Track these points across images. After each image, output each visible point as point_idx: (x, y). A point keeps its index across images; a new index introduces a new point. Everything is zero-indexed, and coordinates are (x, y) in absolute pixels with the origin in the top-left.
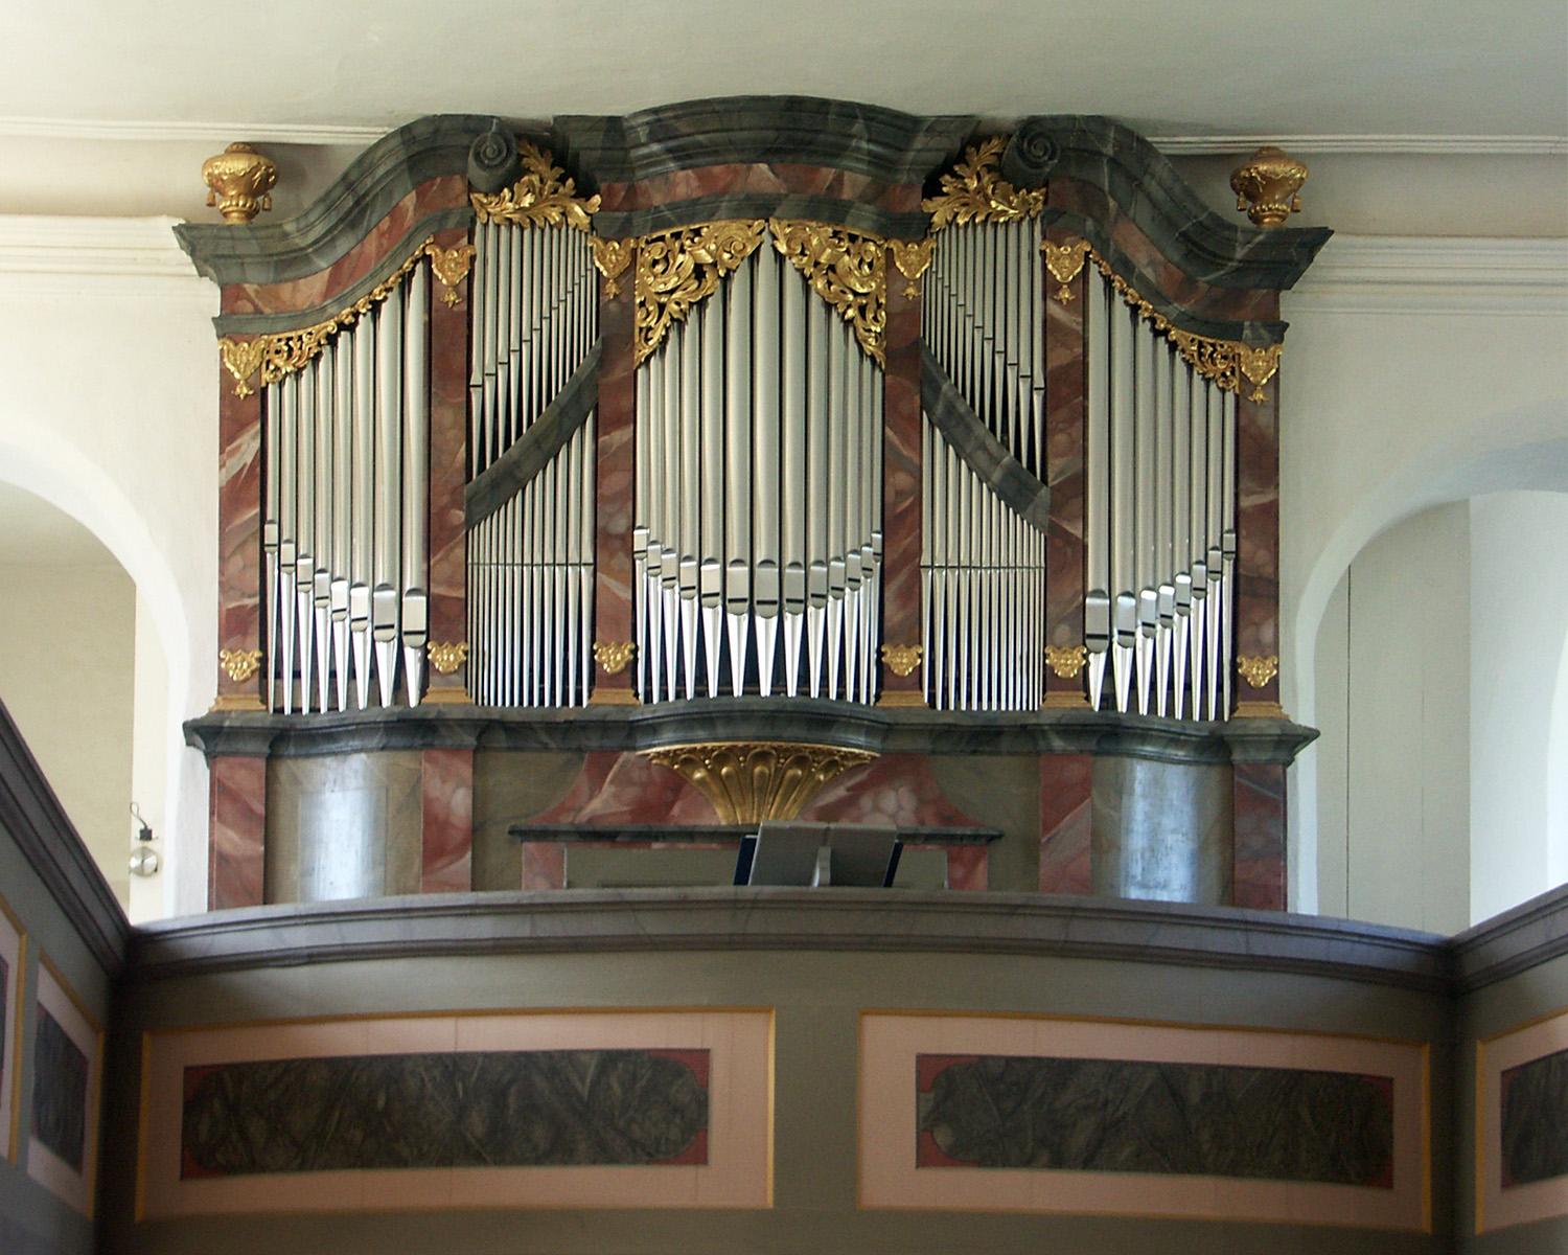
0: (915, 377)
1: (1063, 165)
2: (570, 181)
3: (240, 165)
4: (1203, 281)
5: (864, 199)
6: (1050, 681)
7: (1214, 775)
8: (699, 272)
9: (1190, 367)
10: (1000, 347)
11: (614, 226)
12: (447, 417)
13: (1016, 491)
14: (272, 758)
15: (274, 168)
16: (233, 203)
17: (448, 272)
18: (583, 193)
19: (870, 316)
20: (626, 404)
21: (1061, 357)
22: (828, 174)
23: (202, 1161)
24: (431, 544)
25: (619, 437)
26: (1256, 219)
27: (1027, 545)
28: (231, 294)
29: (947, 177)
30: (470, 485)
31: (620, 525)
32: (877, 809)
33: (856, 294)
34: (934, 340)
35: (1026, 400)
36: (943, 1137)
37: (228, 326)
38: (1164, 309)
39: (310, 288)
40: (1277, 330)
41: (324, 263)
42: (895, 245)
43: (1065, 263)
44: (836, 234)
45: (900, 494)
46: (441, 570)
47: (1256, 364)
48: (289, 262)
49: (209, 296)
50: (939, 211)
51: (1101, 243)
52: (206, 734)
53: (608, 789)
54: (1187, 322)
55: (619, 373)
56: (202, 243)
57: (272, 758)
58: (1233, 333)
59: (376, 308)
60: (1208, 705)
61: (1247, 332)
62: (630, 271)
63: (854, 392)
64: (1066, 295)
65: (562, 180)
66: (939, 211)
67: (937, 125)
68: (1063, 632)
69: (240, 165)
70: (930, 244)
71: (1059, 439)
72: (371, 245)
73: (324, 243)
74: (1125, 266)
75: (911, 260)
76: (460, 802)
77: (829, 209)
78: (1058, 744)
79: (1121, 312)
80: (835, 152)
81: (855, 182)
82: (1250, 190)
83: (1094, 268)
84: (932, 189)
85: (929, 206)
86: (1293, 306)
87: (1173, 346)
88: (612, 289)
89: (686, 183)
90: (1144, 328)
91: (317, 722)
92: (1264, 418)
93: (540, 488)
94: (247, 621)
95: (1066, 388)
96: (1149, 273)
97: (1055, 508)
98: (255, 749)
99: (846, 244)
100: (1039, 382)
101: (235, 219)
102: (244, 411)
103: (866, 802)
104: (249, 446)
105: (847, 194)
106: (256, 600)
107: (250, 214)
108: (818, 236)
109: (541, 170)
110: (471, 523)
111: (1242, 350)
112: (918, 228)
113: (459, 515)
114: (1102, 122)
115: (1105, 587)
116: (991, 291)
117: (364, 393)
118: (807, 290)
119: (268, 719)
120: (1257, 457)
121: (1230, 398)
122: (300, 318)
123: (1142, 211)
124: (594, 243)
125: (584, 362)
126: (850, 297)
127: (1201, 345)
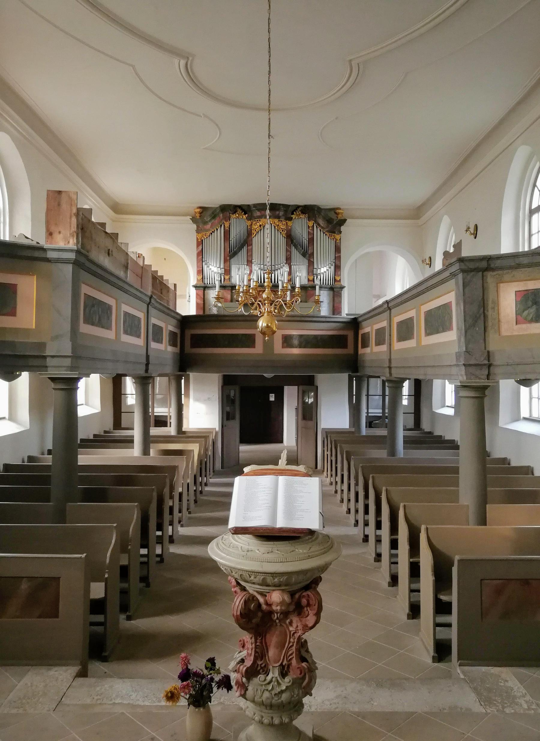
0: (291, 239)
1: (310, 211)
3: (199, 210)
5: (283, 215)
6: (309, 280)
8: (260, 226)
11: (249, 219)
12: (227, 245)
13: (304, 255)
14: (204, 290)
15: (203, 210)
16: (198, 215)
17: (227, 224)
18: (245, 214)
21: (310, 237)
22: (277, 212)
24: (225, 261)
25: (250, 248)
26: (337, 217)
27: (306, 261)
28: (198, 227)
30: (230, 254)
34: (293, 234)
35: (306, 242)
37: (198, 231)
39: (208, 226)
41: (210, 223)
43: (311, 224)
46: (226, 265)
47: (338, 237)
48: (205, 223)
49: (195, 226)
51: (316, 221)
52: (196, 287)
54: (328, 231)
55: (250, 239)
56: (194, 220)
57: (204, 290)
59: (217, 229)
63: (282, 241)
68: (310, 274)
69: (199, 210)
71: (310, 248)
72: (216, 221)
73: (211, 220)
74: (319, 224)
75: (290, 223)
76: (229, 297)
80: (279, 210)
81: (281, 213)
82: (336, 213)
84: (293, 214)
85: (292, 216)
86: (343, 228)
88: (249, 227)
89: (258, 214)
90: (322, 232)
91: (210, 286)
92: (339, 244)
93: (239, 254)
94: (201, 271)
95: (311, 241)
97: (310, 257)
101: (198, 217)
102: (200, 243)
104: (200, 247)
107: (200, 216)
109: (239, 211)
110: (230, 259)
112: (290, 219)
113: (228, 258)
116: (300, 226)
119: (203, 285)
122: (207, 230)
124: (246, 221)
125: (245, 237)
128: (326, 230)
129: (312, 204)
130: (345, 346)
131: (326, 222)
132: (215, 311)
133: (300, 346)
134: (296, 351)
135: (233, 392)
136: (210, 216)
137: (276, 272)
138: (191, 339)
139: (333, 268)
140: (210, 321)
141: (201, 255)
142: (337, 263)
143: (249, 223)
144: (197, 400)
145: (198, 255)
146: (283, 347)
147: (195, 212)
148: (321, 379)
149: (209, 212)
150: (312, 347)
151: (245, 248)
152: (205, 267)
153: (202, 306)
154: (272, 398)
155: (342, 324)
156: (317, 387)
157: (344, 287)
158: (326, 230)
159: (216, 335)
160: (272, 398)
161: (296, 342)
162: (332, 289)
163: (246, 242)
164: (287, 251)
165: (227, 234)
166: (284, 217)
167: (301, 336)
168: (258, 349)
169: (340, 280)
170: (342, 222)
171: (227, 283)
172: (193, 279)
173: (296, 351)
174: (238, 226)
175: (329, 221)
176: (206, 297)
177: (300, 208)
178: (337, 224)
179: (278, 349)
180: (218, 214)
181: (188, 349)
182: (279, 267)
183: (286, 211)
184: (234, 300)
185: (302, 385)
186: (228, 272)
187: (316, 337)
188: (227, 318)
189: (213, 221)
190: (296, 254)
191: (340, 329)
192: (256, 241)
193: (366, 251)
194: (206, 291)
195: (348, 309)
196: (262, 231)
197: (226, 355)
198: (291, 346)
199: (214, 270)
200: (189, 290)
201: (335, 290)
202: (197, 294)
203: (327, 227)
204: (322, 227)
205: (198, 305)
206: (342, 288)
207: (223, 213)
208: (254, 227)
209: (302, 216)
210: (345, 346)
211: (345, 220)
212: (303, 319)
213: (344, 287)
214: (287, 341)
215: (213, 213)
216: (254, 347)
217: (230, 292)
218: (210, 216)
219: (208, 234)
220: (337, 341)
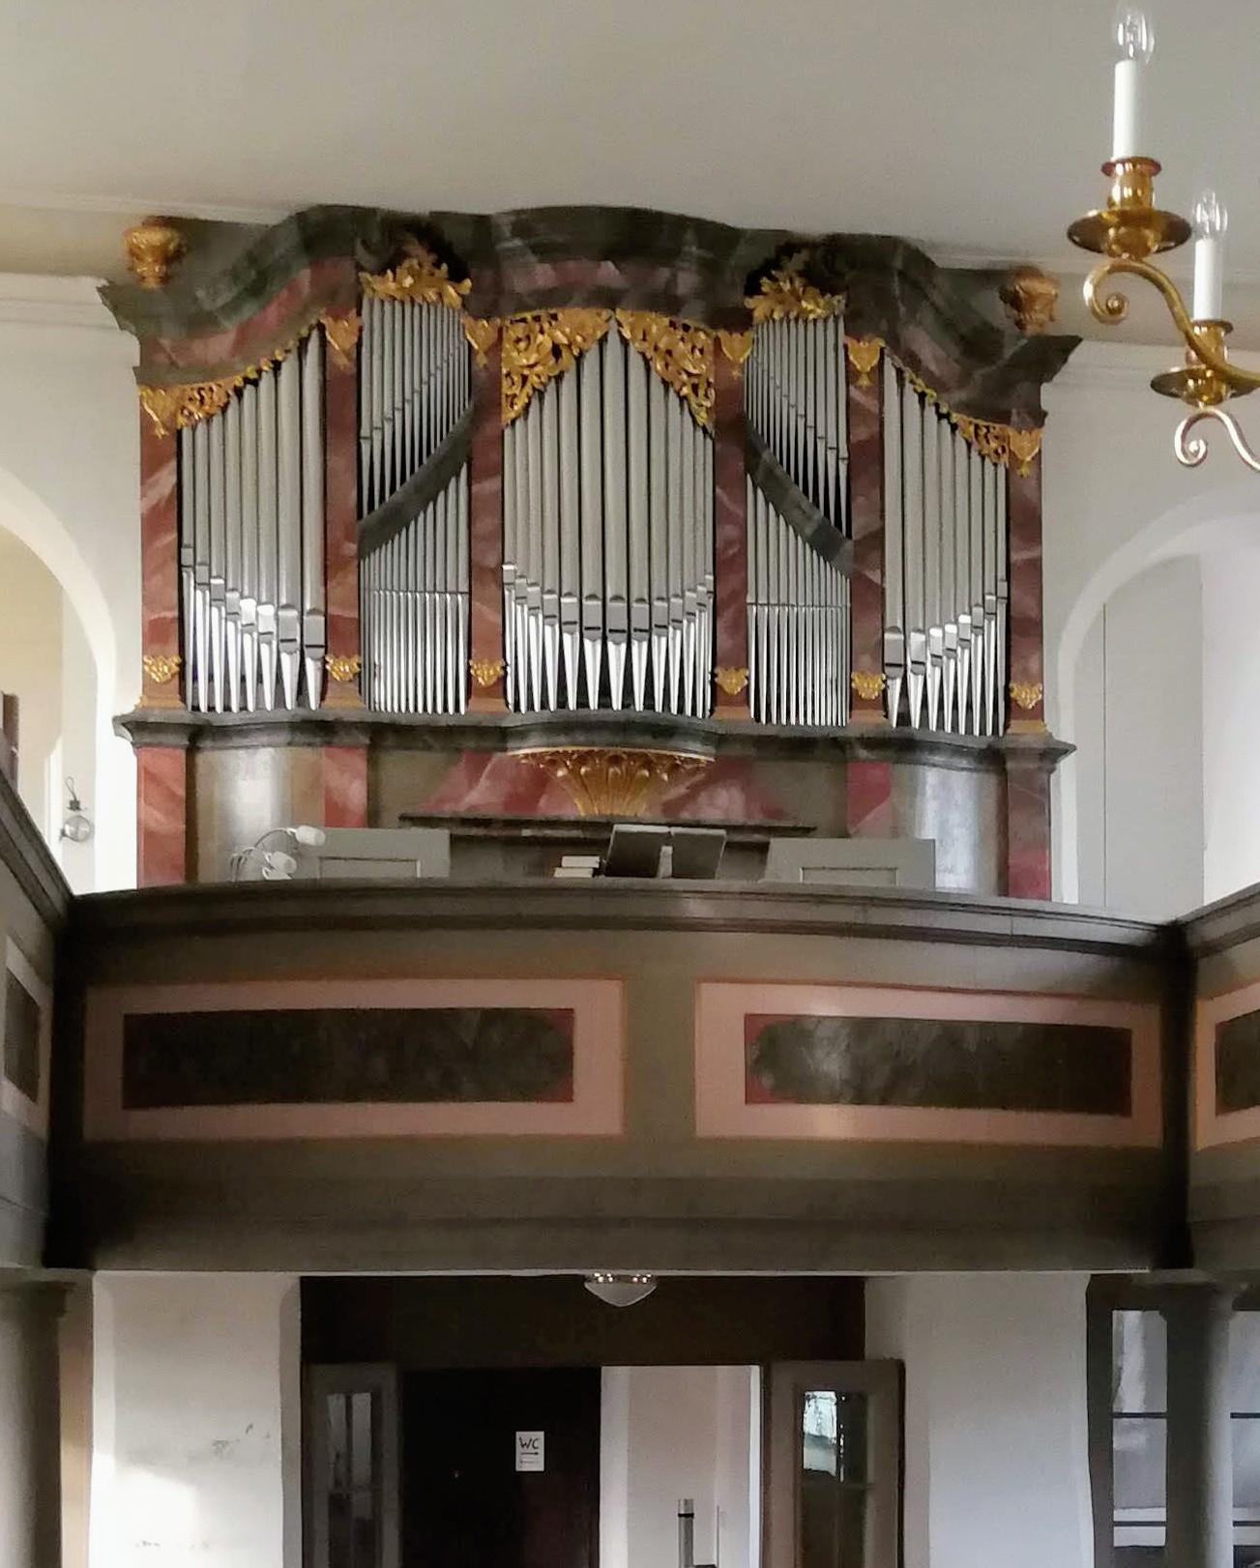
0: (740, 441)
1: (862, 275)
2: (444, 267)
3: (156, 237)
4: (978, 374)
5: (699, 295)
6: (854, 700)
7: (991, 781)
8: (556, 351)
9: (969, 445)
10: (810, 422)
11: (486, 305)
12: (341, 463)
13: (825, 544)
14: (192, 751)
15: (188, 239)
16: (150, 270)
17: (340, 339)
18: (456, 277)
19: (701, 392)
20: (494, 456)
21: (862, 433)
22: (664, 273)
23: (140, 1093)
24: (328, 570)
25: (487, 486)
26: (1020, 324)
27: (835, 586)
28: (149, 348)
29: (764, 280)
30: (364, 522)
31: (491, 561)
32: (711, 804)
33: (689, 374)
34: (756, 415)
35: (832, 465)
36: (767, 1081)
37: (148, 375)
38: (945, 396)
39: (218, 346)
40: (1038, 417)
41: (230, 328)
42: (722, 334)
43: (865, 354)
44: (672, 324)
45: (729, 544)
46: (336, 592)
47: (1022, 443)
48: (200, 323)
49: (128, 347)
50: (759, 306)
51: (894, 341)
52: (136, 727)
53: (484, 782)
54: (966, 408)
55: (489, 430)
56: (124, 301)
57: (192, 751)
58: (1004, 418)
59: (277, 366)
60: (980, 730)
61: (1014, 418)
62: (496, 347)
63: (688, 456)
64: (864, 382)
65: (437, 265)
66: (759, 306)
67: (759, 236)
68: (865, 660)
69: (156, 237)
70: (750, 334)
71: (859, 501)
72: (272, 312)
73: (233, 307)
74: (913, 361)
75: (736, 346)
76: (356, 793)
77: (667, 303)
78: (863, 753)
79: (912, 401)
80: (670, 256)
81: (687, 281)
82: (1014, 301)
83: (887, 360)
84: (753, 289)
85: (750, 303)
86: (1049, 395)
87: (954, 427)
88: (481, 360)
89: (543, 275)
90: (930, 411)
91: (229, 720)
92: (1029, 492)
93: (423, 522)
94: (168, 632)
95: (866, 457)
96: (933, 367)
97: (859, 557)
98: (182, 738)
99: (680, 333)
100: (844, 453)
101: (152, 284)
102: (162, 450)
103: (703, 797)
104: (166, 479)
106: (176, 613)
107: (165, 279)
108: (657, 324)
109: (418, 255)
110: (362, 555)
111: (1011, 432)
112: (742, 321)
113: (352, 548)
115: (900, 625)
117: (267, 440)
118: (648, 370)
119: (187, 717)
120: (1023, 521)
121: (1002, 471)
122: (211, 372)
123: (927, 316)
124: (466, 320)
125: (459, 421)
126: (684, 377)
127: (977, 427)
128: (960, 395)
129: (875, 230)
130: (1112, 1097)
131: (956, 352)
132: (277, 867)
133: (859, 1094)
134: (831, 1122)
135: (358, 1413)
136: (235, 275)
137: (659, 645)
138: (131, 1050)
139: (995, 630)
140: (268, 925)
141: (167, 525)
142: (1023, 602)
143: (481, 333)
144: (139, 1454)
145: (152, 524)
146: (753, 1095)
147: (134, 253)
148: (929, 1312)
149: (225, 257)
150: (925, 1100)
151: (457, 493)
152: (197, 601)
153: (179, 848)
154: (531, 1454)
155: (1079, 960)
156: (900, 1368)
157: (1066, 750)
158: (960, 395)
159: (305, 1021)
160: (531, 1454)
161: (831, 1064)
162: (993, 758)
163: (466, 447)
164: (719, 515)
165: (341, 403)
166: (698, 306)
167: (863, 1028)
168: (594, 1107)
169: (1040, 704)
170: (1051, 354)
171: (344, 706)
172: (114, 674)
173: (831, 1122)
174: (410, 352)
175: (976, 345)
176: (201, 791)
177: (799, 260)
178: (1017, 362)
179: (723, 1105)
180: (286, 269)
181: (106, 1115)
182: (676, 614)
183: (710, 269)
184: (385, 817)
185: (796, 1355)
186: (345, 634)
187: (951, 1032)
188: (386, 907)
189: (249, 310)
190: (776, 547)
191: (1094, 992)
192: (528, 452)
193: (1157, 555)
194: (201, 759)
195: (1103, 875)
196: (568, 386)
197: (377, 1146)
198: (799, 1089)
199: (250, 635)
200: (85, 762)
201: (1014, 769)
202: (147, 778)
203: (963, 381)
204: (934, 382)
205: (148, 838)
206: (1053, 753)
207: (315, 264)
208: (518, 358)
209: (813, 306)
210: (1112, 1097)
211: (1067, 345)
212: (879, 917)
213: (1066, 750)
214: (777, 1056)
215: (252, 259)
216: (567, 1096)
217: (359, 763)
218: (235, 275)
219: (218, 397)
220: (1064, 1065)
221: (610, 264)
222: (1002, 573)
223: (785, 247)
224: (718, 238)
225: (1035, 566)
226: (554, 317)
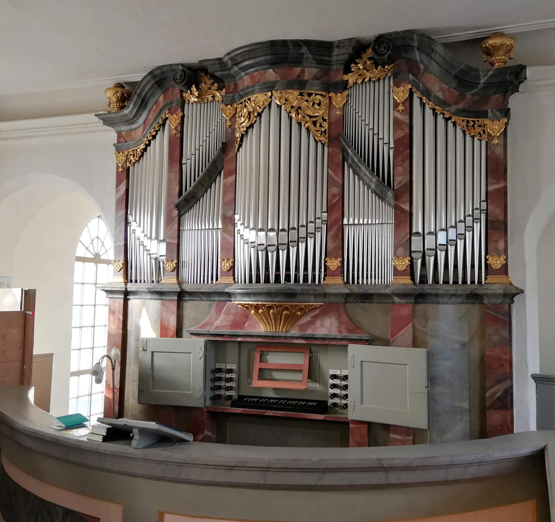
0: (340, 146)
4: (469, 95)
10: (376, 132)
11: (229, 101)
19: (318, 125)
20: (233, 166)
21: (401, 134)
27: (388, 214)
29: (353, 65)
31: (230, 213)
32: (322, 326)
33: (311, 117)
35: (387, 152)
38: (447, 109)
40: (506, 113)
42: (332, 94)
43: (401, 94)
44: (301, 94)
45: (334, 196)
47: (495, 127)
50: (350, 78)
53: (222, 316)
54: (458, 113)
58: (484, 115)
61: (490, 114)
64: (401, 108)
65: (213, 84)
66: (350, 78)
70: (346, 93)
74: (427, 93)
75: (339, 99)
77: (300, 84)
78: (397, 300)
79: (429, 113)
83: (415, 95)
84: (347, 70)
85: (346, 77)
87: (454, 124)
95: (405, 145)
96: (440, 95)
99: (306, 97)
100: (392, 145)
103: (318, 323)
105: (306, 77)
108: (293, 95)
111: (487, 122)
114: (411, 32)
115: (420, 231)
116: (372, 108)
118: (291, 118)
120: (497, 168)
121: (484, 143)
123: (434, 67)
126: (307, 118)
127: (468, 122)
131: (454, 83)
139: (479, 229)
164: (331, 182)
175: (464, 80)
204: (443, 103)
209: (376, 72)
221: (271, 70)
222: (484, 197)
223: (358, 48)
224: (321, 49)
225: (504, 192)
226: (249, 99)
